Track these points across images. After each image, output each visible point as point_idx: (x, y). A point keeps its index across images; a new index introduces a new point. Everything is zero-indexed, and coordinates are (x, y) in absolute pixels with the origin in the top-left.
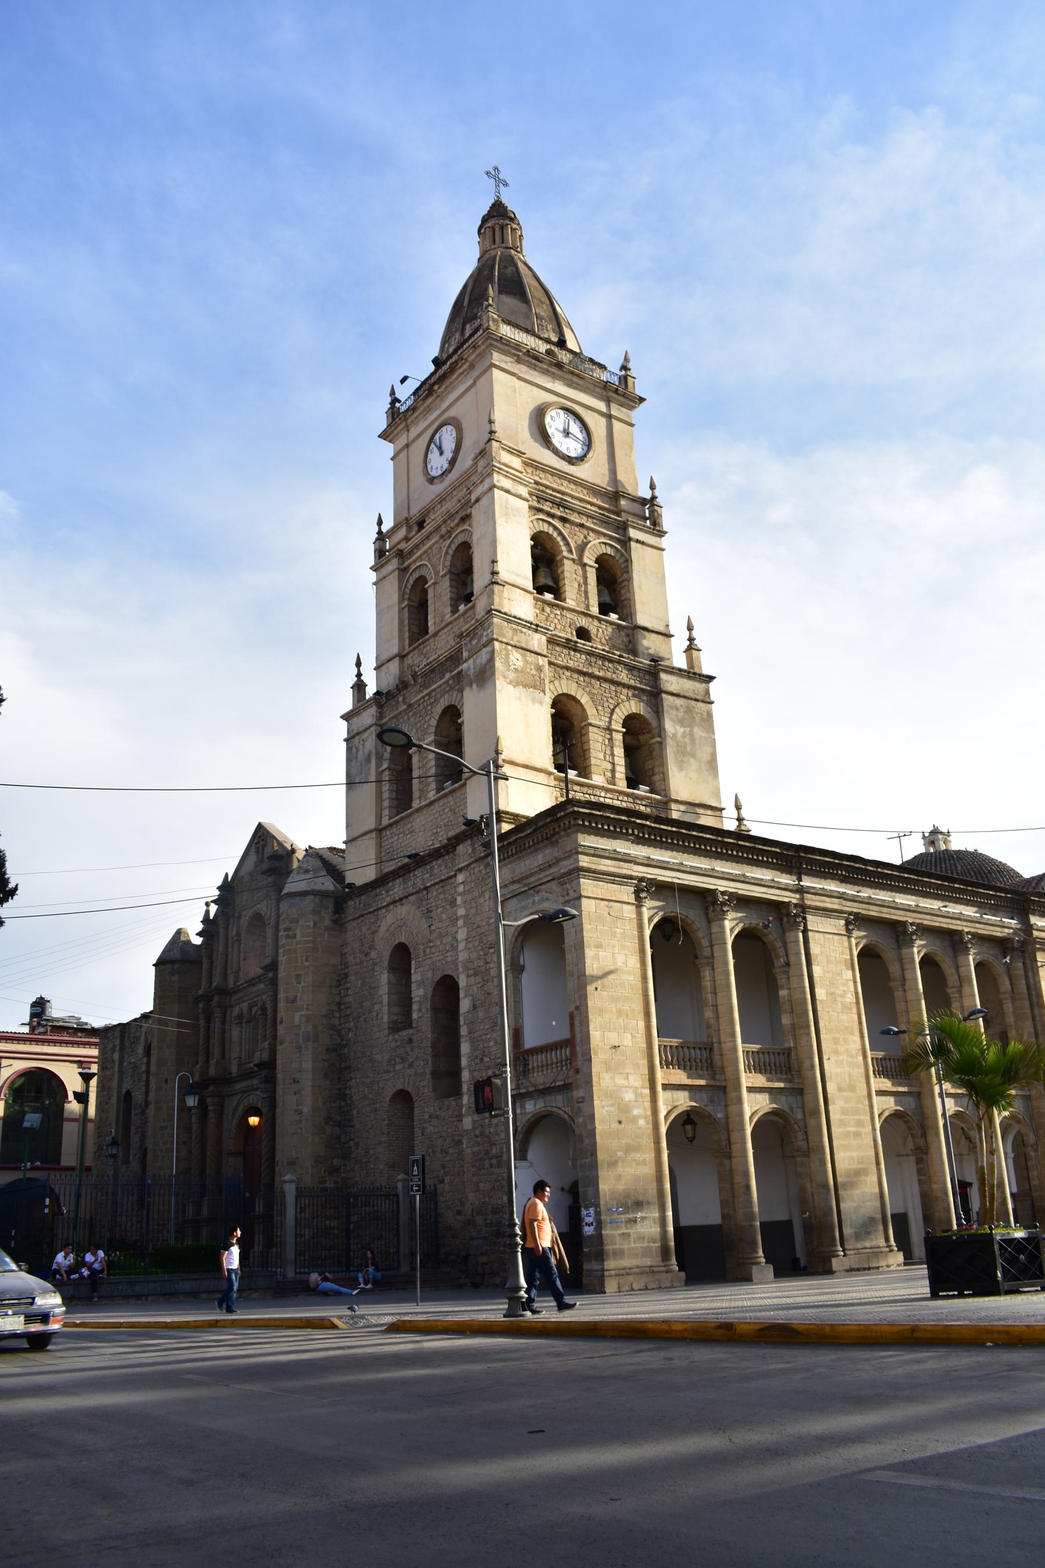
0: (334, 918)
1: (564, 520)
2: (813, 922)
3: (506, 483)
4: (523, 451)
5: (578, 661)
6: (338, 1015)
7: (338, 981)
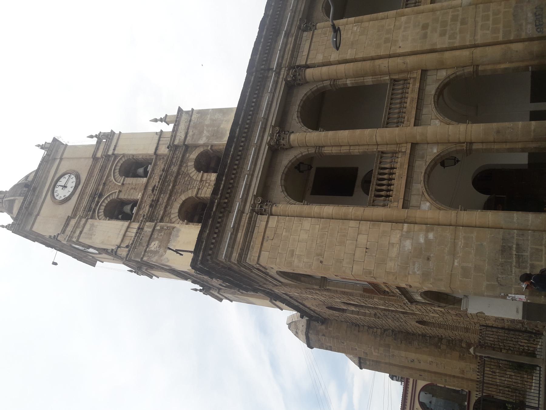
0: (320, 324)
1: (101, 196)
2: (301, 61)
3: (78, 232)
4: (67, 217)
5: (164, 199)
6: (375, 329)
7: (356, 326)
